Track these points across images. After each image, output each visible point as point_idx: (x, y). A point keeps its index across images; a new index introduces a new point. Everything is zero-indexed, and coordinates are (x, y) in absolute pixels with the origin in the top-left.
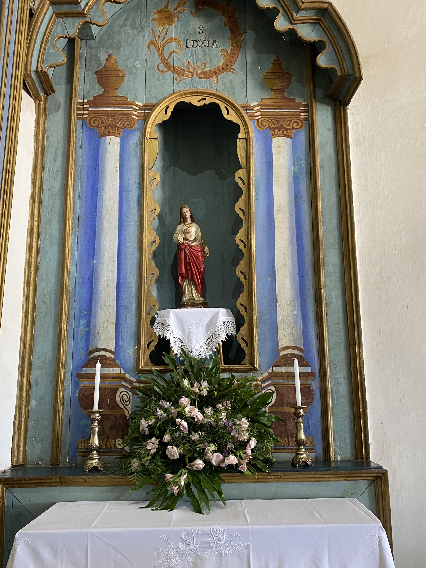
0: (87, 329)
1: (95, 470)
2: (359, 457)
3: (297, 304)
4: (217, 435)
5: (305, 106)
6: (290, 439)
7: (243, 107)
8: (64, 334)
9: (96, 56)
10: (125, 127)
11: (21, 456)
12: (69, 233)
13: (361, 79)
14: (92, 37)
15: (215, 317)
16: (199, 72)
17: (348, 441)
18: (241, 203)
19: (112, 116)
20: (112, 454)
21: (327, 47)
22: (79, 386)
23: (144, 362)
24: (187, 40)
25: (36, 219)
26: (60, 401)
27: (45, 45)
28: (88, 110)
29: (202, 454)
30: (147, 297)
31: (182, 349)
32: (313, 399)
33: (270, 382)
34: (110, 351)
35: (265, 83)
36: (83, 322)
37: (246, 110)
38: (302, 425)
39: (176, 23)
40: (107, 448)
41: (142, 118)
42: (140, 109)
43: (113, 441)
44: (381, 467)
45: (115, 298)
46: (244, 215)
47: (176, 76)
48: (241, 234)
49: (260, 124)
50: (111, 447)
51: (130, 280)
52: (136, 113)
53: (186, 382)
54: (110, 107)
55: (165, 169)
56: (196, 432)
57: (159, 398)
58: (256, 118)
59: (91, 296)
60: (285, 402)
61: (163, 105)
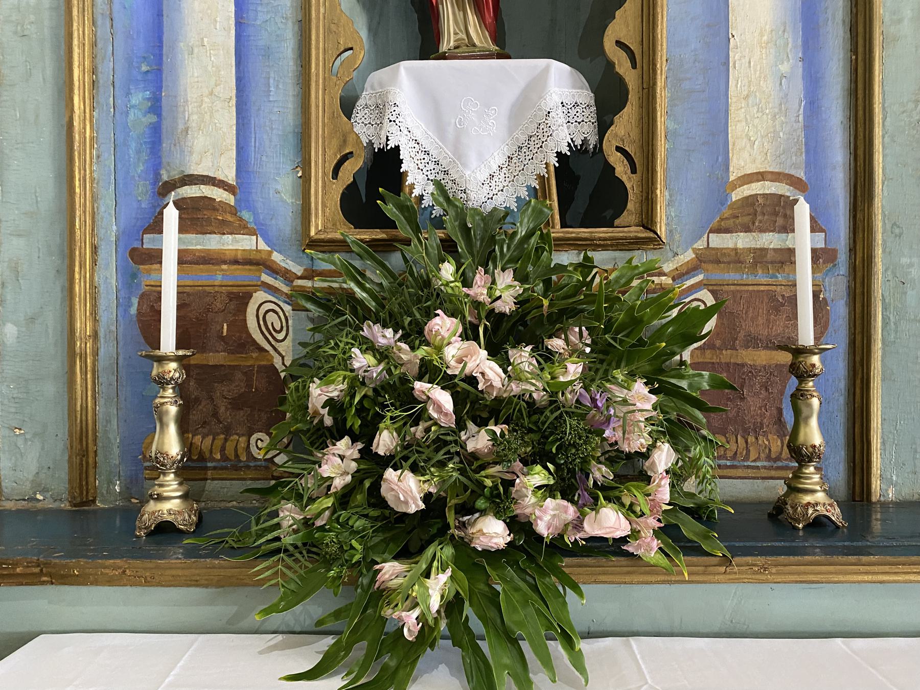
0: (153, 118)
1: (165, 530)
3: (792, 41)
4: (552, 436)
6: (751, 439)
15: (538, 84)
22: (138, 285)
23: (327, 218)
26: (83, 326)
29: (501, 500)
31: (438, 184)
33: (700, 277)
36: (139, 98)
38: (815, 402)
40: (224, 458)
43: (243, 440)
45: (232, 22)
50: (237, 456)
53: (448, 270)
56: (481, 423)
57: (363, 314)
59: (160, 14)
60: (742, 335)
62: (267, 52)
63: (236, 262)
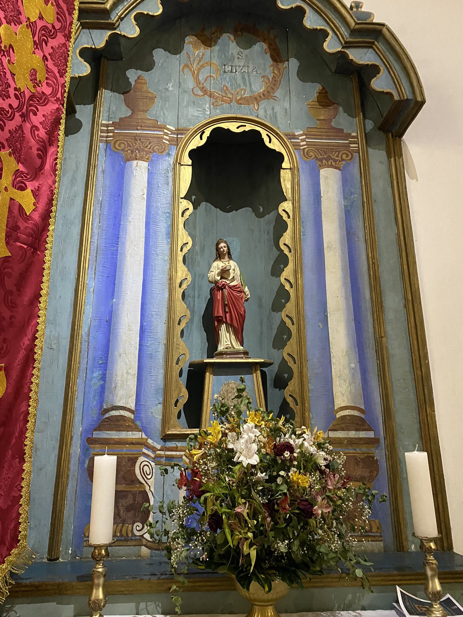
7: (286, 135)
13: (423, 102)
16: (238, 98)
19: (140, 140)
20: (129, 543)
22: (89, 454)
24: (225, 65)
28: (114, 132)
32: (378, 472)
34: (129, 410)
37: (290, 139)
40: (121, 535)
42: (172, 133)
43: (130, 526)
45: (138, 344)
46: (290, 251)
49: (306, 154)
50: (127, 534)
52: (168, 138)
54: (137, 130)
58: (301, 148)
59: (108, 341)
62: (151, 356)
63: (133, 444)
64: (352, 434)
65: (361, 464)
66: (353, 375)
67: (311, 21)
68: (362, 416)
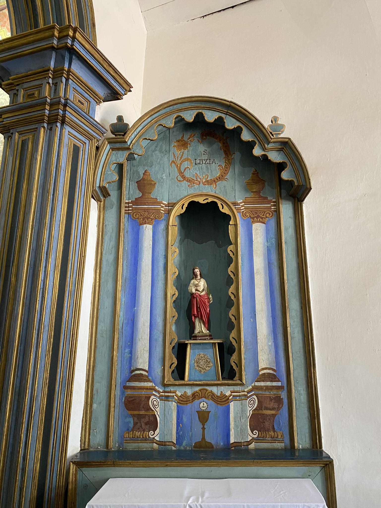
0: (130, 355)
2: (315, 447)
3: (271, 337)
5: (274, 202)
6: (267, 433)
7: (232, 204)
8: (115, 358)
9: (137, 171)
10: (156, 218)
11: (87, 443)
12: (119, 290)
13: (311, 189)
14: (134, 159)
16: (204, 181)
17: (307, 435)
18: (231, 268)
20: (147, 442)
21: (288, 166)
24: (196, 160)
25: (98, 280)
27: (105, 169)
28: (132, 207)
30: (170, 333)
33: (253, 393)
35: (247, 187)
36: (127, 350)
37: (235, 205)
39: (189, 148)
40: (143, 437)
41: (167, 212)
42: (166, 206)
43: (147, 433)
44: (329, 457)
46: (234, 276)
47: (189, 184)
48: (232, 289)
49: (244, 215)
51: (158, 321)
52: (163, 209)
54: (146, 205)
55: (181, 242)
59: (133, 332)
61: (180, 204)
62: (156, 340)
63: (147, 389)
64: (269, 384)
65: (273, 401)
66: (270, 350)
67: (246, 136)
68: (275, 373)
